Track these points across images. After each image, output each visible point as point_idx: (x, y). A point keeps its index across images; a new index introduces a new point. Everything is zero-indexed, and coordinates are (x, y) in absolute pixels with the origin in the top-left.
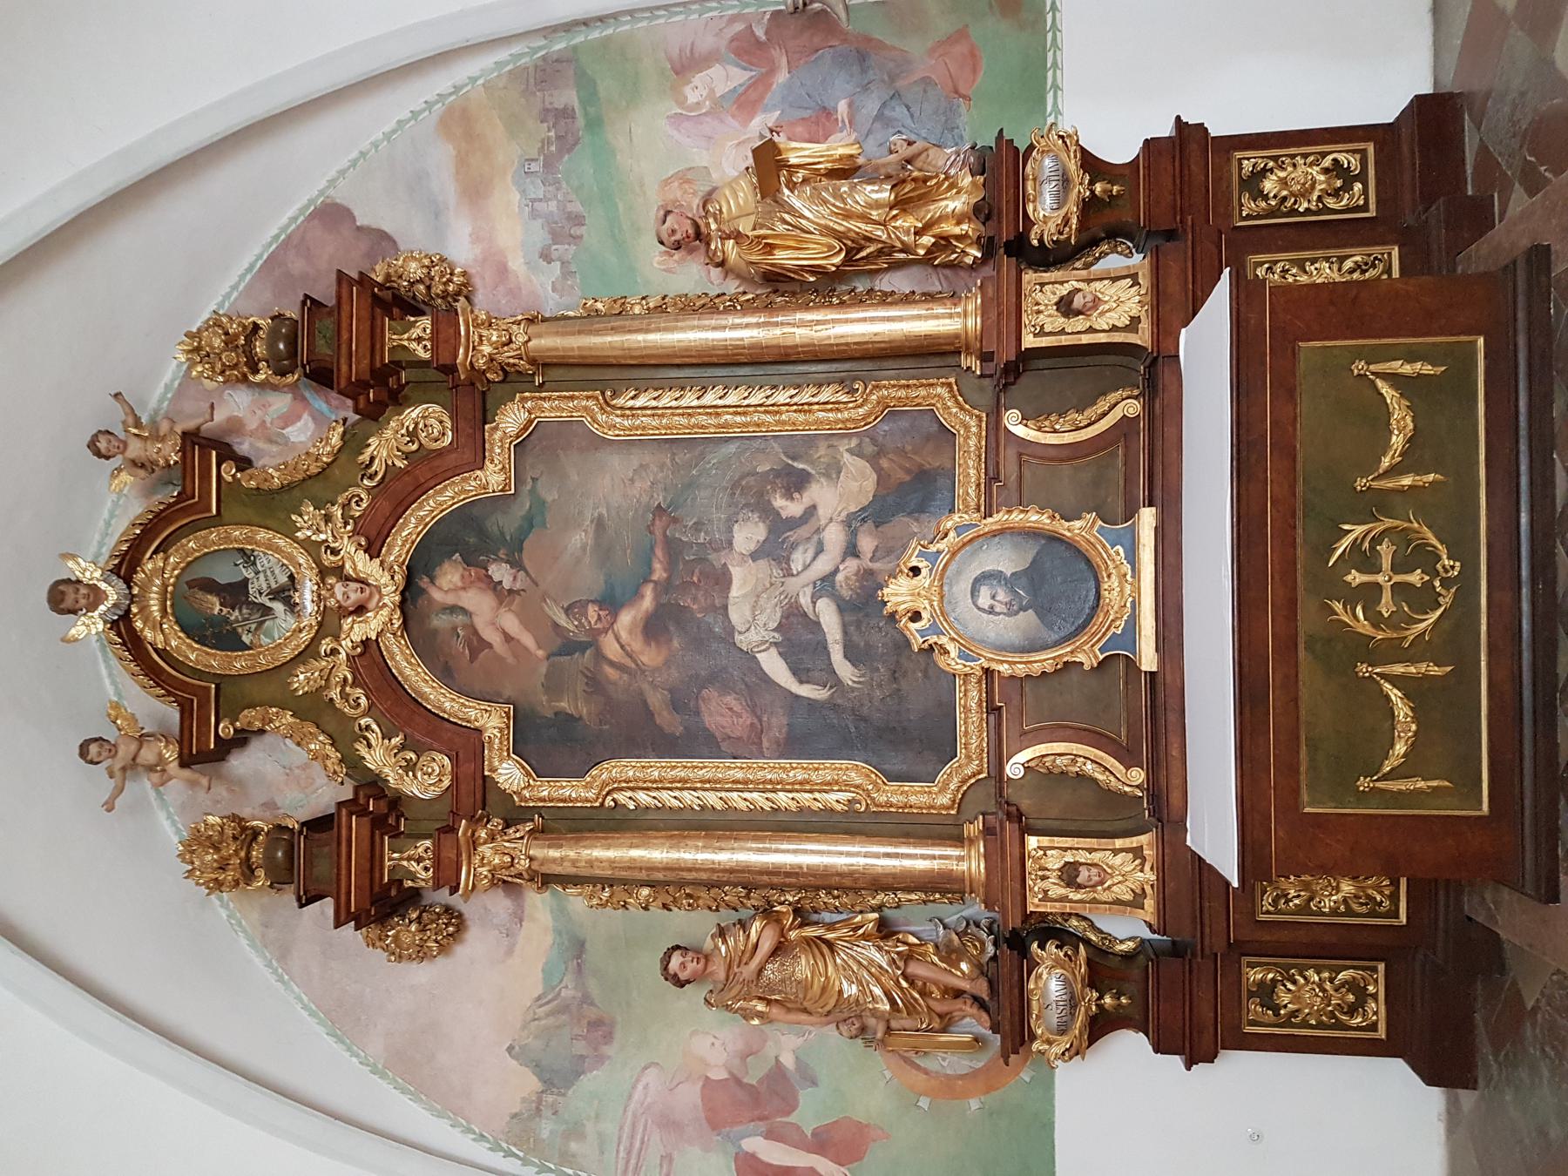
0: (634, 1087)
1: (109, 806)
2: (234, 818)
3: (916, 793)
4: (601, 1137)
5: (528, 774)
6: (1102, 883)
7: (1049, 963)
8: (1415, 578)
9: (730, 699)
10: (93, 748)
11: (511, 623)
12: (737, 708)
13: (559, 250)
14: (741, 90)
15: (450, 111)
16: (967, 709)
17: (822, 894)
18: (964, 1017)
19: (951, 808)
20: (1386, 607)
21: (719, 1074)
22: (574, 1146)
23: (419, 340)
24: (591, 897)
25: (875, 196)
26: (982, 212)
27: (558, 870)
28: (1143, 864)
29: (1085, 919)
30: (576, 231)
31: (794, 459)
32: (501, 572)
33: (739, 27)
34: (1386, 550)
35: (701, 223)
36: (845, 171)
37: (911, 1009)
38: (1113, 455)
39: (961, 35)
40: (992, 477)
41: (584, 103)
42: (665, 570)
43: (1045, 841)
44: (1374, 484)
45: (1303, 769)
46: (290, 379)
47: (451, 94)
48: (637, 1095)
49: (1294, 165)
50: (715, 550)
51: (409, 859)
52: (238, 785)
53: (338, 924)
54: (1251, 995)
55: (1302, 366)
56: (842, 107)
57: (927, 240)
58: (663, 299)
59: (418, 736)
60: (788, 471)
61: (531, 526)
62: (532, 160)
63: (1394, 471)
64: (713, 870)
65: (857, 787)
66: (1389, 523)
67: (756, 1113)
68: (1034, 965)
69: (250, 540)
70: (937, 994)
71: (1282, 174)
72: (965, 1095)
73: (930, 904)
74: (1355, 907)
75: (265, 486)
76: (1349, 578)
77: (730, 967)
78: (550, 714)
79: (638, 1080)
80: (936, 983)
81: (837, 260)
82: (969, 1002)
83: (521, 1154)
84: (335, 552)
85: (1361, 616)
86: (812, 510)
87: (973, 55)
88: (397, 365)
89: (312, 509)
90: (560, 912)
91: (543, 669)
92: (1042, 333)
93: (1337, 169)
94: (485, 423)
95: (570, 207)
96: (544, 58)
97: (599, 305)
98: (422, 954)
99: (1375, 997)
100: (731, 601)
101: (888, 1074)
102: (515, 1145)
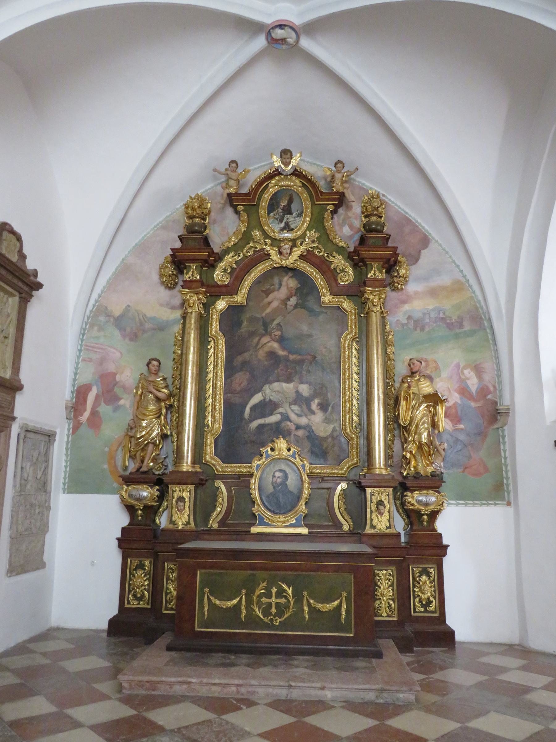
0: (115, 349)
1: (215, 170)
2: (209, 213)
3: (210, 448)
4: (98, 338)
5: (221, 311)
6: (178, 510)
7: (152, 492)
8: (274, 610)
9: (245, 383)
11: (275, 304)
12: (242, 385)
14: (468, 389)
17: (177, 415)
18: (135, 464)
19: (205, 461)
20: (264, 600)
21: (118, 378)
22: (96, 328)
24: (178, 333)
25: (423, 436)
26: (417, 476)
27: (187, 322)
31: (333, 407)
32: (293, 301)
33: (492, 389)
34: (283, 601)
35: (417, 374)
36: (434, 425)
37: (138, 444)
38: (330, 521)
39: (486, 470)
40: (322, 478)
41: (465, 331)
42: (293, 359)
43: (193, 492)
45: (212, 571)
47: (469, 284)
49: (431, 587)
50: (300, 378)
51: (193, 272)
53: (172, 249)
54: (141, 561)
56: (462, 426)
57: (408, 456)
58: (393, 360)
59: (235, 273)
60: (328, 405)
61: (310, 312)
62: (444, 313)
63: (309, 605)
64: (185, 376)
65: (213, 427)
66: (292, 602)
68: (152, 487)
69: (306, 215)
70: (142, 454)
71: (428, 582)
73: (173, 454)
75: (325, 220)
76: (274, 588)
77: (153, 382)
79: (117, 350)
80: (146, 454)
81: (402, 423)
82: (140, 465)
83: (94, 310)
84: (301, 244)
85: (262, 591)
86: (313, 413)
91: (258, 316)
94: (347, 296)
95: (427, 327)
96: (481, 318)
97: (390, 337)
98: (161, 276)
100: (281, 383)
101: (116, 437)
102: (97, 308)
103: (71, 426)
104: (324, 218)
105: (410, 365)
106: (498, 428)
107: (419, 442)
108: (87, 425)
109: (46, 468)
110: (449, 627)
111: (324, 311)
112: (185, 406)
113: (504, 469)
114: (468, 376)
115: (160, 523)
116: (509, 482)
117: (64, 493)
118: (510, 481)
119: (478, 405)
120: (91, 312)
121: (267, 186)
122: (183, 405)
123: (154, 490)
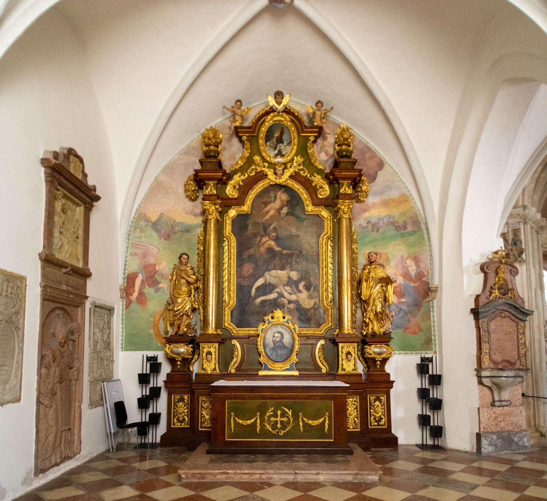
0: (153, 246)
1: (224, 107)
2: (221, 141)
3: (228, 318)
4: (140, 237)
5: (232, 217)
6: (207, 361)
7: (188, 349)
8: (279, 426)
9: (251, 270)
10: (239, 103)
11: (272, 213)
12: (249, 272)
13: (370, 226)
14: (409, 274)
15: (407, 197)
16: (249, 331)
17: (202, 294)
18: (173, 329)
20: (272, 419)
21: (157, 268)
22: (138, 230)
23: (345, 190)
24: (201, 234)
25: (378, 307)
26: (374, 335)
27: (208, 226)
29: (198, 359)
30: (375, 230)
31: (314, 287)
32: (285, 210)
33: (426, 273)
34: (285, 419)
35: (374, 263)
36: (385, 299)
37: (175, 316)
38: (313, 366)
39: (421, 330)
40: (308, 337)
41: (408, 232)
43: (217, 348)
44: (300, 417)
46: (336, 155)
48: (152, 247)
49: (382, 409)
50: (290, 267)
51: (211, 188)
52: (230, 139)
54: (181, 396)
55: (328, 401)
56: (404, 300)
57: (367, 321)
59: (242, 189)
60: (311, 286)
63: (303, 421)
64: (208, 266)
65: (229, 303)
67: (148, 278)
68: (187, 345)
69: (294, 144)
70: (178, 322)
71: (380, 406)
72: (154, 329)
74: (203, 419)
75: (308, 148)
76: (279, 411)
77: (184, 270)
78: (248, 223)
80: (181, 322)
81: (363, 298)
84: (291, 167)
86: (300, 292)
87: (415, 333)
88: (339, 183)
89: (302, 160)
90: (197, 226)
91: (260, 221)
92: (342, 348)
93: (381, 419)
94: (325, 206)
95: (381, 229)
96: (420, 222)
97: (355, 236)
98: (186, 191)
99: (181, 425)
100: (277, 271)
101: (158, 310)
103: (124, 303)
104: (307, 146)
105: (369, 257)
106: (429, 301)
107: (375, 311)
108: (136, 302)
109: (109, 333)
110: (394, 435)
111: (308, 217)
113: (432, 329)
114: (409, 264)
116: (436, 338)
117: (122, 351)
118: (437, 337)
119: (416, 285)
120: (134, 218)
121: (264, 121)
122: (207, 287)
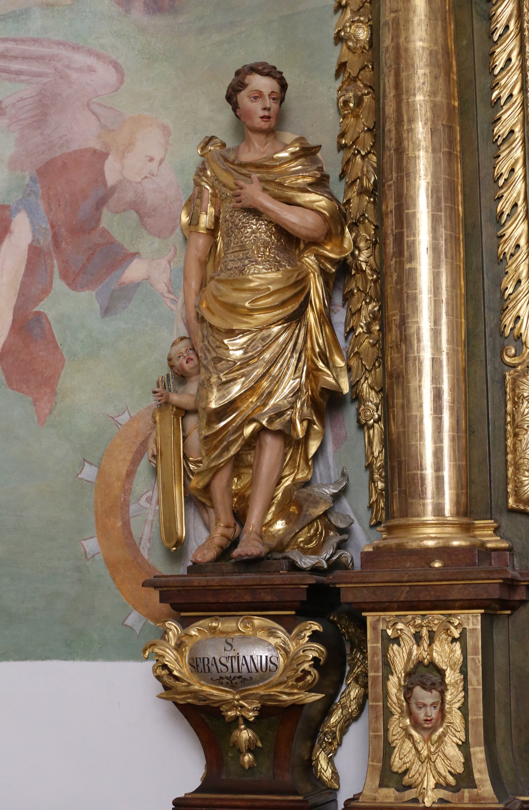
0: (90, 52)
6: (416, 724)
7: (292, 647)
17: (373, 307)
18: (208, 528)
19: (518, 499)
28: (448, 787)
29: (361, 708)
64: (399, 122)
67: (63, 231)
70: (237, 485)
73: (366, 475)
77: (257, 166)
79: (99, 56)
80: (252, 484)
82: (230, 532)
101: (124, 418)
112: (412, 258)
115: (335, 773)
122: (400, 253)
123: (298, 636)
